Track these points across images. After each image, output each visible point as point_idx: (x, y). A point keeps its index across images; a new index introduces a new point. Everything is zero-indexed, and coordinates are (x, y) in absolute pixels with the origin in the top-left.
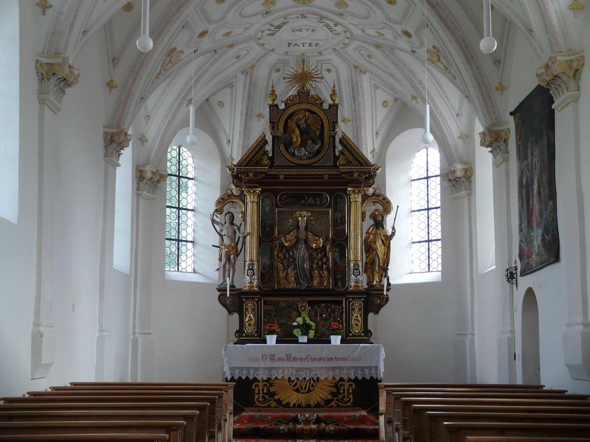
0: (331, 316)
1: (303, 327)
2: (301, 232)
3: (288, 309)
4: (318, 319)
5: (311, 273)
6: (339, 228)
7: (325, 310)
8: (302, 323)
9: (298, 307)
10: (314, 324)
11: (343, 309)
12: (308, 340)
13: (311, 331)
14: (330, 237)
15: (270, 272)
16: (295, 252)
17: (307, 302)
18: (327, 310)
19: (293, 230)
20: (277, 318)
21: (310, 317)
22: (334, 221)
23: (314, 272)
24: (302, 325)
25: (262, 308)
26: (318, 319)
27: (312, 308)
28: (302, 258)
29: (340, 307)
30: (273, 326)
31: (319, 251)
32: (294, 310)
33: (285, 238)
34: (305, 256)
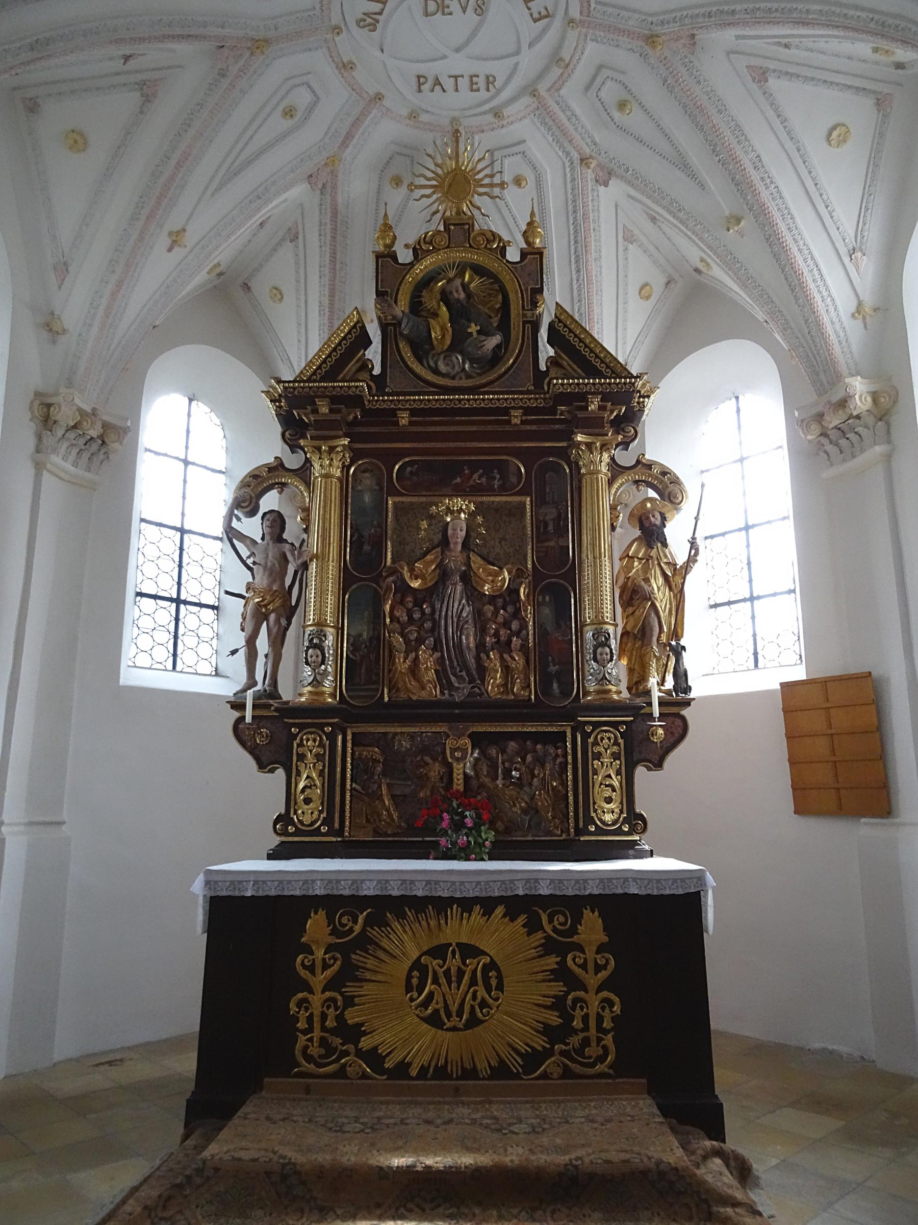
0: (533, 776)
2: (454, 554)
4: (500, 782)
5: (478, 659)
6: (552, 544)
9: (444, 753)
14: (529, 566)
15: (372, 657)
16: (438, 606)
17: (469, 736)
18: (524, 760)
19: (434, 548)
22: (538, 528)
23: (488, 657)
26: (500, 782)
27: (483, 753)
28: (455, 620)
31: (500, 602)
32: (435, 759)
33: (412, 570)
34: (464, 615)
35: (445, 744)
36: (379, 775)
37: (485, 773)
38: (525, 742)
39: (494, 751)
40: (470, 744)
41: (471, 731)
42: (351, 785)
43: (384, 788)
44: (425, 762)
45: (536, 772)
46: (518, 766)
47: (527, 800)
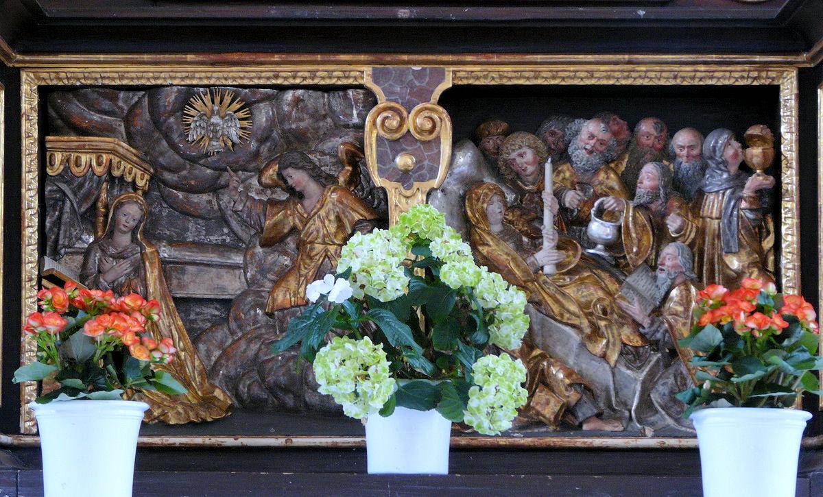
0: (661, 235)
1: (412, 322)
3: (272, 172)
4: (547, 256)
7: (613, 181)
8: (396, 285)
9: (356, 156)
10: (518, 299)
11: (774, 167)
12: (454, 450)
13: (489, 360)
18: (629, 185)
20: (166, 252)
21: (469, 230)
24: (400, 307)
25: (29, 162)
26: (547, 256)
27: (491, 161)
29: (756, 153)
30: (100, 310)
32: (325, 180)
35: (360, 127)
36: (134, 231)
37: (496, 228)
38: (632, 128)
39: (529, 155)
40: (448, 124)
41: (447, 84)
42: (40, 263)
43: (152, 275)
44: (291, 190)
45: (673, 223)
46: (610, 202)
47: (639, 318)
